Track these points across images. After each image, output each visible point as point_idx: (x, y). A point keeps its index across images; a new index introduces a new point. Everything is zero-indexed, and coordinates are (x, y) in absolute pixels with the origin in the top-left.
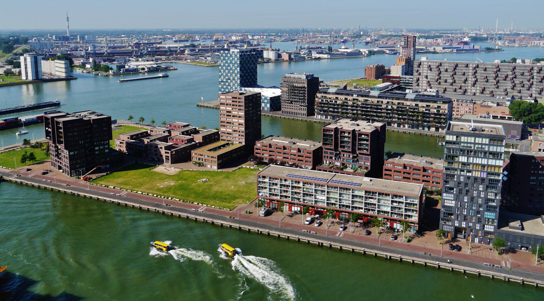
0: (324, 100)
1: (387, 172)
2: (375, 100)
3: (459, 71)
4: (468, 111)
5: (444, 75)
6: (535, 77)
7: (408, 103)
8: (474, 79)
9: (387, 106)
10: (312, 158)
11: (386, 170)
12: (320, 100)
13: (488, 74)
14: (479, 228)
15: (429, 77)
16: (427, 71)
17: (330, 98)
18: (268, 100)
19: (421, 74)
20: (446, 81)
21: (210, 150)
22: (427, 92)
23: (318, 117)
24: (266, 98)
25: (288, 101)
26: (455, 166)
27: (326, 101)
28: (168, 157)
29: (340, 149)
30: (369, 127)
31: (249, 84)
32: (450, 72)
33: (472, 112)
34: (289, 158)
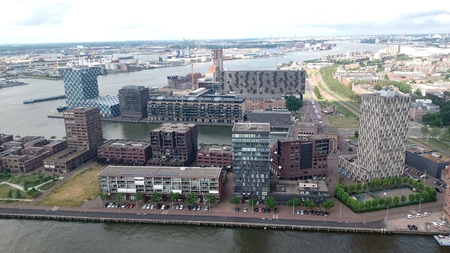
0: (154, 106)
1: (199, 160)
2: (192, 104)
3: (250, 78)
4: (257, 106)
5: (241, 81)
6: (300, 79)
7: (216, 104)
8: (260, 83)
9: (201, 107)
10: (144, 155)
11: (198, 158)
12: (151, 106)
13: (270, 78)
14: (258, 194)
15: (230, 82)
16: (229, 78)
17: (158, 104)
18: (110, 108)
19: (225, 80)
20: (242, 85)
21: (61, 158)
22: (230, 94)
23: (151, 118)
24: (107, 107)
25: (125, 108)
26: (240, 154)
27: (155, 106)
28: (23, 167)
29: (164, 147)
30: (185, 128)
31: (92, 96)
32: (244, 78)
33: (260, 106)
34: (127, 157)
